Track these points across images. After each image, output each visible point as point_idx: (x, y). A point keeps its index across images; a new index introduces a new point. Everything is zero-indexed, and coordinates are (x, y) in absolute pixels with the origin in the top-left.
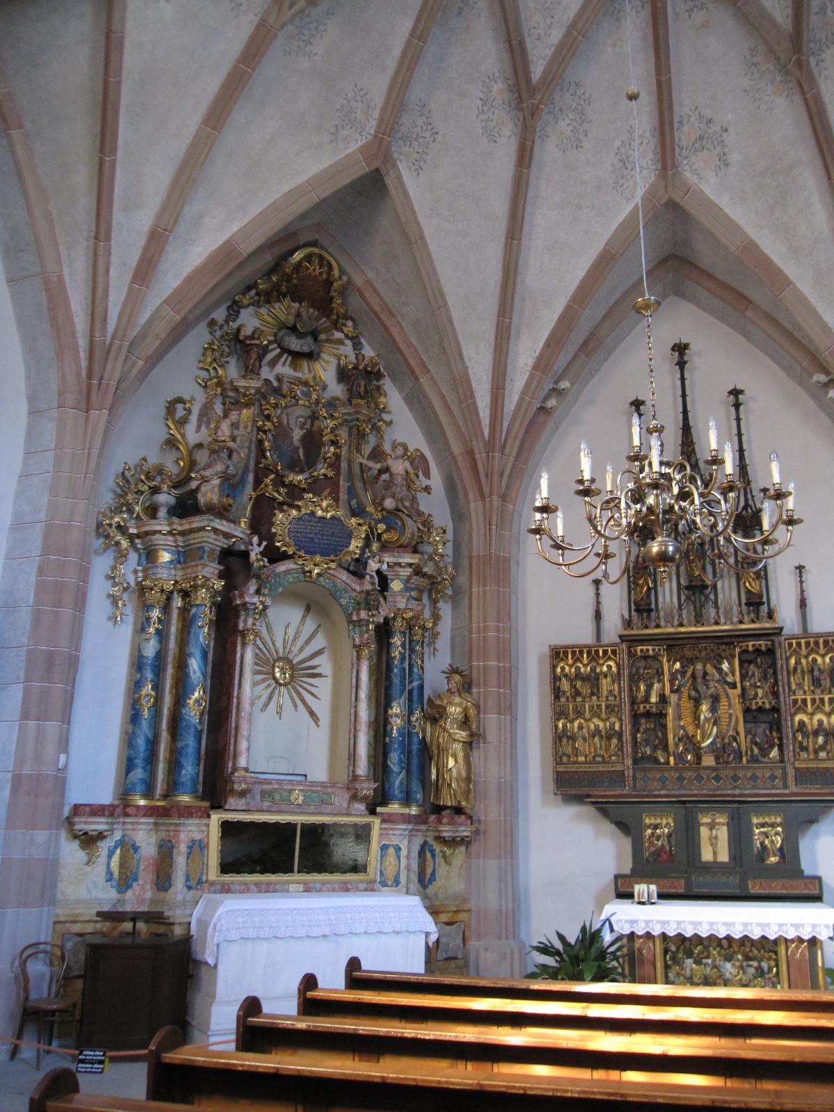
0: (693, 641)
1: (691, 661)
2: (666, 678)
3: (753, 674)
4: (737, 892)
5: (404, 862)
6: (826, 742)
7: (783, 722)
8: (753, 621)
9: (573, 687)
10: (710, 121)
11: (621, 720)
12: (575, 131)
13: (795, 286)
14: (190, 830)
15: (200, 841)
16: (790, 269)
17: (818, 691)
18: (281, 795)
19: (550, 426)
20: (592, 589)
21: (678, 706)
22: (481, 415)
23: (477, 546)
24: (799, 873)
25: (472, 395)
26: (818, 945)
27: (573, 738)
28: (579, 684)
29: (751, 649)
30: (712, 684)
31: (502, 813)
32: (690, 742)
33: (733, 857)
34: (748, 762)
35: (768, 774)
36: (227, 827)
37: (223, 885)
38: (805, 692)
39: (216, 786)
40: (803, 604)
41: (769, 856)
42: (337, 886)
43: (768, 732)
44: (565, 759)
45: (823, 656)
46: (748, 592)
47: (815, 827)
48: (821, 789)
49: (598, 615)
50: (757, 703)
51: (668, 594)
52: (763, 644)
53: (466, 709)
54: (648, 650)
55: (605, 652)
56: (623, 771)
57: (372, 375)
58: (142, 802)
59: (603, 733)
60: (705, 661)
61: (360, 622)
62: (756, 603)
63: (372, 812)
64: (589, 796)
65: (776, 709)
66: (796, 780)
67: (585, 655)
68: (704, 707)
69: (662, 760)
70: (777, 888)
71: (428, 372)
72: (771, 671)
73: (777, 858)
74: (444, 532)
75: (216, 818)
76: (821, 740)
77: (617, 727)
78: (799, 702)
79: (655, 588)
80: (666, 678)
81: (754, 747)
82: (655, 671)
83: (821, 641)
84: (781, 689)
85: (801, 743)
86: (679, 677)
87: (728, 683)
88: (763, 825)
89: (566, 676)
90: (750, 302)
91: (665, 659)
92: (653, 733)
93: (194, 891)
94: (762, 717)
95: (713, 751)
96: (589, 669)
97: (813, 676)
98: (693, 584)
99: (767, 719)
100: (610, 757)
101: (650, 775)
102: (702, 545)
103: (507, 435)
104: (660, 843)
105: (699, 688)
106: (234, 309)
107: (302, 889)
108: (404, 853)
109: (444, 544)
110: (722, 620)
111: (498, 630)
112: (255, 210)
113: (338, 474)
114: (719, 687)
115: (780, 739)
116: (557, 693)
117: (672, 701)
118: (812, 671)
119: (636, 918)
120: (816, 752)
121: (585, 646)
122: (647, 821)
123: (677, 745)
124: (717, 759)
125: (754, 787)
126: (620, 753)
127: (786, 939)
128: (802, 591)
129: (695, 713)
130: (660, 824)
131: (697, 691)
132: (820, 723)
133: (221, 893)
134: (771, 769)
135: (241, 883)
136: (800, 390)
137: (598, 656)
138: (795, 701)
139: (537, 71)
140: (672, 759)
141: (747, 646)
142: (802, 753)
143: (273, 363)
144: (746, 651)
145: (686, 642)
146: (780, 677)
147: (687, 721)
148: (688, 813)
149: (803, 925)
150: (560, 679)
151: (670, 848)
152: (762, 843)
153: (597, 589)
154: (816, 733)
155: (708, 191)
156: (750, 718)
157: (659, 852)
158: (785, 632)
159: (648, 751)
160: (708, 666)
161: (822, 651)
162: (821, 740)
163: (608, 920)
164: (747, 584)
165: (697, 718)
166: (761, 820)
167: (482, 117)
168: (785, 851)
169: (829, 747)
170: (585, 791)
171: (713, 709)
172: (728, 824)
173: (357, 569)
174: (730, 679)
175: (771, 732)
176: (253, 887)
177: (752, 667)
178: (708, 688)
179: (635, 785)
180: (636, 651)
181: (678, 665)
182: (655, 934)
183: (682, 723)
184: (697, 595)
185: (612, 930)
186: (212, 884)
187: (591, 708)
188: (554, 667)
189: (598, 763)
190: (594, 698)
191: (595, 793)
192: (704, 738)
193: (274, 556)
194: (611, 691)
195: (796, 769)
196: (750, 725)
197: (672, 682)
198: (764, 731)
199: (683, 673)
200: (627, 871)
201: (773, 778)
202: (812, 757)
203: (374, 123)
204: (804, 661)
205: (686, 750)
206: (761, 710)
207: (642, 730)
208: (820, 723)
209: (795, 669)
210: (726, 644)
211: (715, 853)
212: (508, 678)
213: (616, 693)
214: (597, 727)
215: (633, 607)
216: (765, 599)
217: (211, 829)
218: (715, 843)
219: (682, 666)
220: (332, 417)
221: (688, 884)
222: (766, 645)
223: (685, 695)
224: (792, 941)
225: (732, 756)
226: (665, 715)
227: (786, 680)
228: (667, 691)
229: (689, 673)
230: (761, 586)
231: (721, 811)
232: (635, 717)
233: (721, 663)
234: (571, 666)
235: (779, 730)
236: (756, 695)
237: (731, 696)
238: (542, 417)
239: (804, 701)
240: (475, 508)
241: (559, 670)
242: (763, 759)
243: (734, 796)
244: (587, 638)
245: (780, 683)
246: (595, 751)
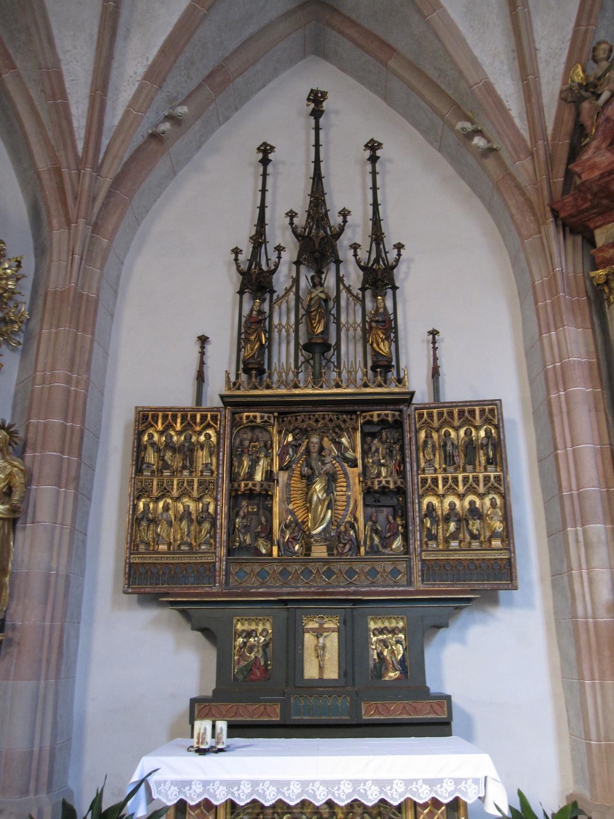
0: (309, 408)
1: (305, 433)
2: (276, 449)
3: (377, 450)
4: (346, 718)
6: (458, 529)
7: (410, 506)
8: (380, 386)
11: (216, 500)
13: (445, 11)
17: (451, 469)
19: (162, 166)
20: (197, 348)
21: (288, 485)
22: (75, 124)
23: (56, 280)
24: (421, 692)
26: (462, 811)
27: (154, 521)
28: (168, 455)
29: (375, 419)
30: (328, 459)
31: (48, 617)
32: (298, 529)
33: (344, 671)
34: (367, 553)
35: (389, 568)
38: (435, 470)
40: (435, 372)
41: (387, 670)
43: (391, 518)
44: (142, 548)
45: (457, 429)
46: (376, 354)
47: (442, 632)
48: (452, 585)
49: (201, 377)
50: (380, 482)
51: (283, 355)
52: (389, 414)
54: (255, 417)
55: (204, 418)
56: (214, 563)
59: (194, 517)
60: (322, 434)
64: (166, 594)
65: (401, 491)
66: (422, 576)
67: (179, 420)
68: (318, 487)
69: (264, 551)
70: (397, 711)
71: (14, 68)
72: (398, 447)
73: (398, 673)
74: (19, 265)
76: (452, 526)
77: (211, 509)
78: (429, 481)
79: (270, 347)
80: (276, 449)
81: (374, 535)
82: (262, 444)
83: (456, 411)
84: (408, 466)
85: (429, 530)
86: (291, 451)
87: (346, 460)
88: (381, 631)
89: (153, 444)
90: (392, 50)
91: (275, 431)
92: (254, 517)
94: (385, 500)
95: (326, 540)
96: (182, 438)
97: (445, 451)
98: (313, 341)
99: (390, 501)
100: (199, 546)
101: (247, 569)
102: (326, 301)
103: (106, 153)
104: (253, 656)
105: (313, 464)
109: (18, 279)
110: (344, 385)
111: (69, 381)
114: (337, 465)
115: (405, 527)
116: (139, 464)
117: (280, 480)
118: (445, 445)
119: (186, 777)
120: (447, 541)
121: (180, 410)
122: (239, 627)
123: (282, 532)
124: (330, 549)
125: (372, 584)
126: (212, 541)
127: (415, 804)
128: (435, 359)
129: (307, 493)
130: (255, 631)
131: (311, 468)
132: (452, 506)
134: (394, 561)
136: (438, 155)
137: (195, 423)
138: (424, 481)
140: (275, 549)
141: (372, 416)
142: (430, 542)
144: (369, 423)
145: (301, 408)
146: (407, 452)
147: (296, 506)
149: (440, 781)
150: (145, 448)
151: (266, 662)
152: (380, 654)
153: (203, 347)
154: (447, 519)
156: (370, 501)
157: (250, 669)
158: (416, 400)
159: (248, 539)
160: (326, 439)
161: (456, 423)
162: (452, 526)
163: (143, 780)
164: (375, 345)
165: (308, 499)
166: (380, 625)
168: (407, 664)
169: (461, 535)
170: (163, 588)
171: (328, 490)
172: (339, 630)
174: (350, 454)
175: (394, 519)
177: (376, 441)
178: (324, 464)
179: (227, 583)
180: (241, 418)
181: (290, 438)
182: (216, 803)
183: (291, 507)
184: (317, 356)
185: (150, 799)
187: (181, 484)
188: (139, 434)
189: (184, 553)
190: (186, 473)
191: (176, 590)
192: (315, 526)
194: (207, 464)
195: (423, 561)
196: (370, 510)
197: (281, 457)
198: (387, 518)
199: (296, 447)
200: (210, 694)
201: (395, 572)
202: (441, 547)
204: (435, 435)
205: (294, 539)
206: (384, 491)
207: (242, 514)
208: (452, 506)
209: (425, 442)
210: (347, 413)
211: (321, 668)
212: (79, 445)
213: (214, 468)
214: (186, 508)
215: (242, 366)
216: (394, 363)
218: (321, 655)
219: (294, 439)
221: (285, 712)
222: (394, 415)
223: (297, 472)
224: (425, 806)
225: (348, 547)
226: (272, 497)
227: (414, 456)
228: (276, 468)
229: (303, 448)
230: (390, 348)
232: (235, 497)
233: (340, 437)
234: (161, 433)
235: (404, 516)
236: (379, 475)
237: (350, 476)
238: (153, 146)
239: (435, 481)
240: (58, 236)
241: (146, 438)
242: (383, 550)
243: (348, 593)
244: (186, 400)
245: (408, 460)
246: (182, 538)
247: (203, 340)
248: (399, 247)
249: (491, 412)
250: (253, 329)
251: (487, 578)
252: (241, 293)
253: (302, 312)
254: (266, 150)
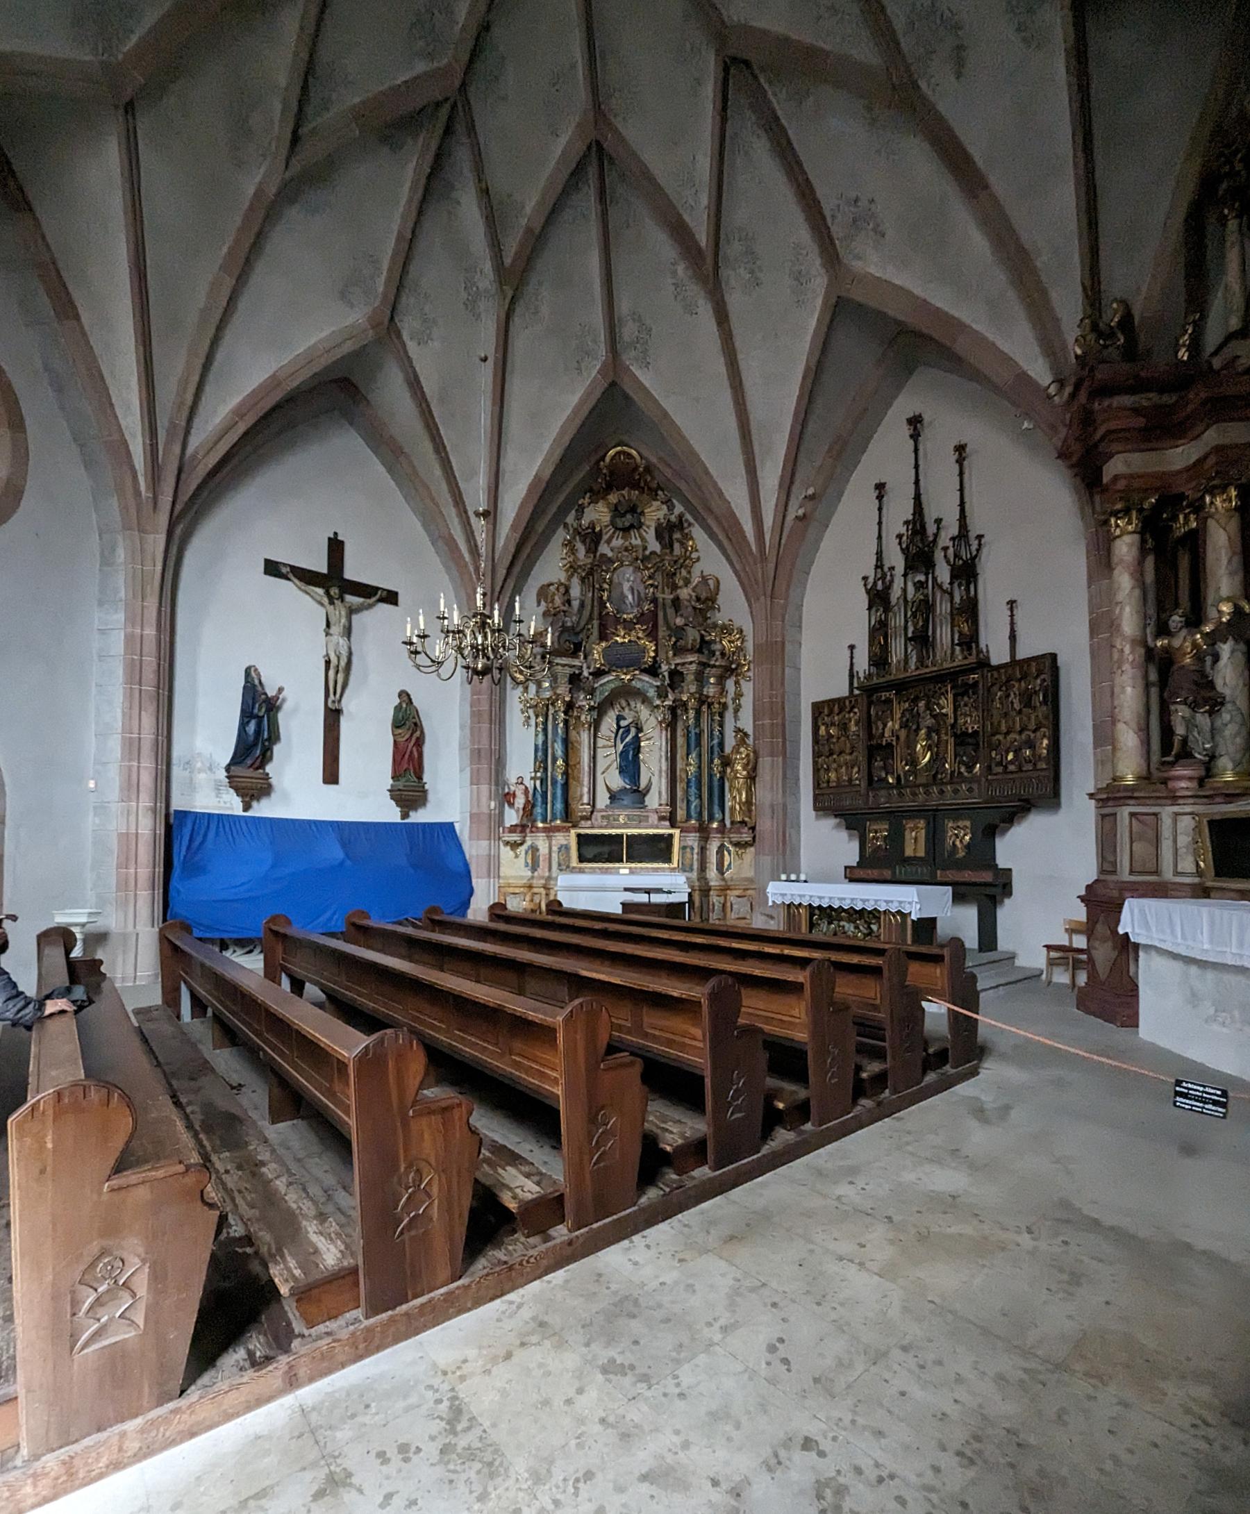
5: (695, 856)
9: (827, 732)
10: (856, 201)
12: (752, 272)
14: (559, 839)
16: (962, 313)
20: (848, 653)
25: (737, 523)
36: (579, 836)
39: (567, 814)
51: (898, 649)
53: (748, 755)
57: (680, 525)
58: (540, 825)
61: (657, 707)
62: (969, 641)
63: (673, 826)
75: (573, 832)
106: (581, 510)
108: (696, 851)
112: (546, 447)
113: (656, 607)
139: (703, 239)
143: (609, 542)
148: (897, 818)
155: (872, 270)
167: (679, 298)
173: (653, 671)
193: (598, 674)
203: (603, 346)
206: (965, 734)
218: (915, 842)
220: (648, 569)
231: (920, 818)
247: (852, 647)
248: (980, 537)
249: (1049, 664)
250: (879, 632)
251: (1044, 793)
252: (869, 609)
253: (909, 613)
254: (880, 487)
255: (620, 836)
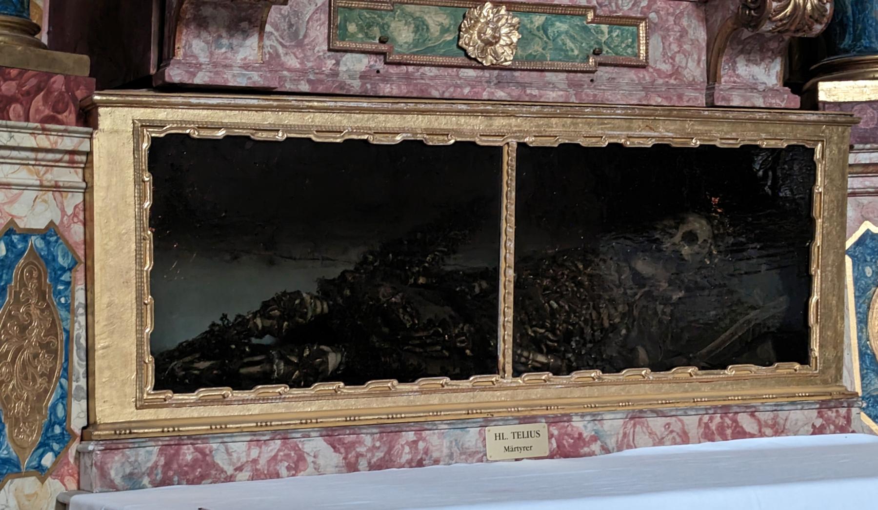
15: (50, 233)
18: (420, 27)
37: (173, 440)
42: (691, 422)
75: (120, 129)
93: (30, 484)
107: (543, 446)
133: (165, 482)
135: (259, 432)
176: (315, 446)
186: (122, 438)
217: (100, 180)
255: (479, 159)
